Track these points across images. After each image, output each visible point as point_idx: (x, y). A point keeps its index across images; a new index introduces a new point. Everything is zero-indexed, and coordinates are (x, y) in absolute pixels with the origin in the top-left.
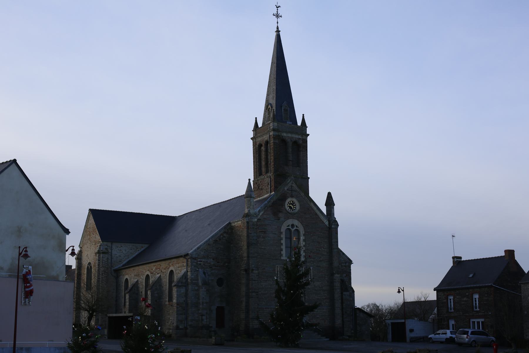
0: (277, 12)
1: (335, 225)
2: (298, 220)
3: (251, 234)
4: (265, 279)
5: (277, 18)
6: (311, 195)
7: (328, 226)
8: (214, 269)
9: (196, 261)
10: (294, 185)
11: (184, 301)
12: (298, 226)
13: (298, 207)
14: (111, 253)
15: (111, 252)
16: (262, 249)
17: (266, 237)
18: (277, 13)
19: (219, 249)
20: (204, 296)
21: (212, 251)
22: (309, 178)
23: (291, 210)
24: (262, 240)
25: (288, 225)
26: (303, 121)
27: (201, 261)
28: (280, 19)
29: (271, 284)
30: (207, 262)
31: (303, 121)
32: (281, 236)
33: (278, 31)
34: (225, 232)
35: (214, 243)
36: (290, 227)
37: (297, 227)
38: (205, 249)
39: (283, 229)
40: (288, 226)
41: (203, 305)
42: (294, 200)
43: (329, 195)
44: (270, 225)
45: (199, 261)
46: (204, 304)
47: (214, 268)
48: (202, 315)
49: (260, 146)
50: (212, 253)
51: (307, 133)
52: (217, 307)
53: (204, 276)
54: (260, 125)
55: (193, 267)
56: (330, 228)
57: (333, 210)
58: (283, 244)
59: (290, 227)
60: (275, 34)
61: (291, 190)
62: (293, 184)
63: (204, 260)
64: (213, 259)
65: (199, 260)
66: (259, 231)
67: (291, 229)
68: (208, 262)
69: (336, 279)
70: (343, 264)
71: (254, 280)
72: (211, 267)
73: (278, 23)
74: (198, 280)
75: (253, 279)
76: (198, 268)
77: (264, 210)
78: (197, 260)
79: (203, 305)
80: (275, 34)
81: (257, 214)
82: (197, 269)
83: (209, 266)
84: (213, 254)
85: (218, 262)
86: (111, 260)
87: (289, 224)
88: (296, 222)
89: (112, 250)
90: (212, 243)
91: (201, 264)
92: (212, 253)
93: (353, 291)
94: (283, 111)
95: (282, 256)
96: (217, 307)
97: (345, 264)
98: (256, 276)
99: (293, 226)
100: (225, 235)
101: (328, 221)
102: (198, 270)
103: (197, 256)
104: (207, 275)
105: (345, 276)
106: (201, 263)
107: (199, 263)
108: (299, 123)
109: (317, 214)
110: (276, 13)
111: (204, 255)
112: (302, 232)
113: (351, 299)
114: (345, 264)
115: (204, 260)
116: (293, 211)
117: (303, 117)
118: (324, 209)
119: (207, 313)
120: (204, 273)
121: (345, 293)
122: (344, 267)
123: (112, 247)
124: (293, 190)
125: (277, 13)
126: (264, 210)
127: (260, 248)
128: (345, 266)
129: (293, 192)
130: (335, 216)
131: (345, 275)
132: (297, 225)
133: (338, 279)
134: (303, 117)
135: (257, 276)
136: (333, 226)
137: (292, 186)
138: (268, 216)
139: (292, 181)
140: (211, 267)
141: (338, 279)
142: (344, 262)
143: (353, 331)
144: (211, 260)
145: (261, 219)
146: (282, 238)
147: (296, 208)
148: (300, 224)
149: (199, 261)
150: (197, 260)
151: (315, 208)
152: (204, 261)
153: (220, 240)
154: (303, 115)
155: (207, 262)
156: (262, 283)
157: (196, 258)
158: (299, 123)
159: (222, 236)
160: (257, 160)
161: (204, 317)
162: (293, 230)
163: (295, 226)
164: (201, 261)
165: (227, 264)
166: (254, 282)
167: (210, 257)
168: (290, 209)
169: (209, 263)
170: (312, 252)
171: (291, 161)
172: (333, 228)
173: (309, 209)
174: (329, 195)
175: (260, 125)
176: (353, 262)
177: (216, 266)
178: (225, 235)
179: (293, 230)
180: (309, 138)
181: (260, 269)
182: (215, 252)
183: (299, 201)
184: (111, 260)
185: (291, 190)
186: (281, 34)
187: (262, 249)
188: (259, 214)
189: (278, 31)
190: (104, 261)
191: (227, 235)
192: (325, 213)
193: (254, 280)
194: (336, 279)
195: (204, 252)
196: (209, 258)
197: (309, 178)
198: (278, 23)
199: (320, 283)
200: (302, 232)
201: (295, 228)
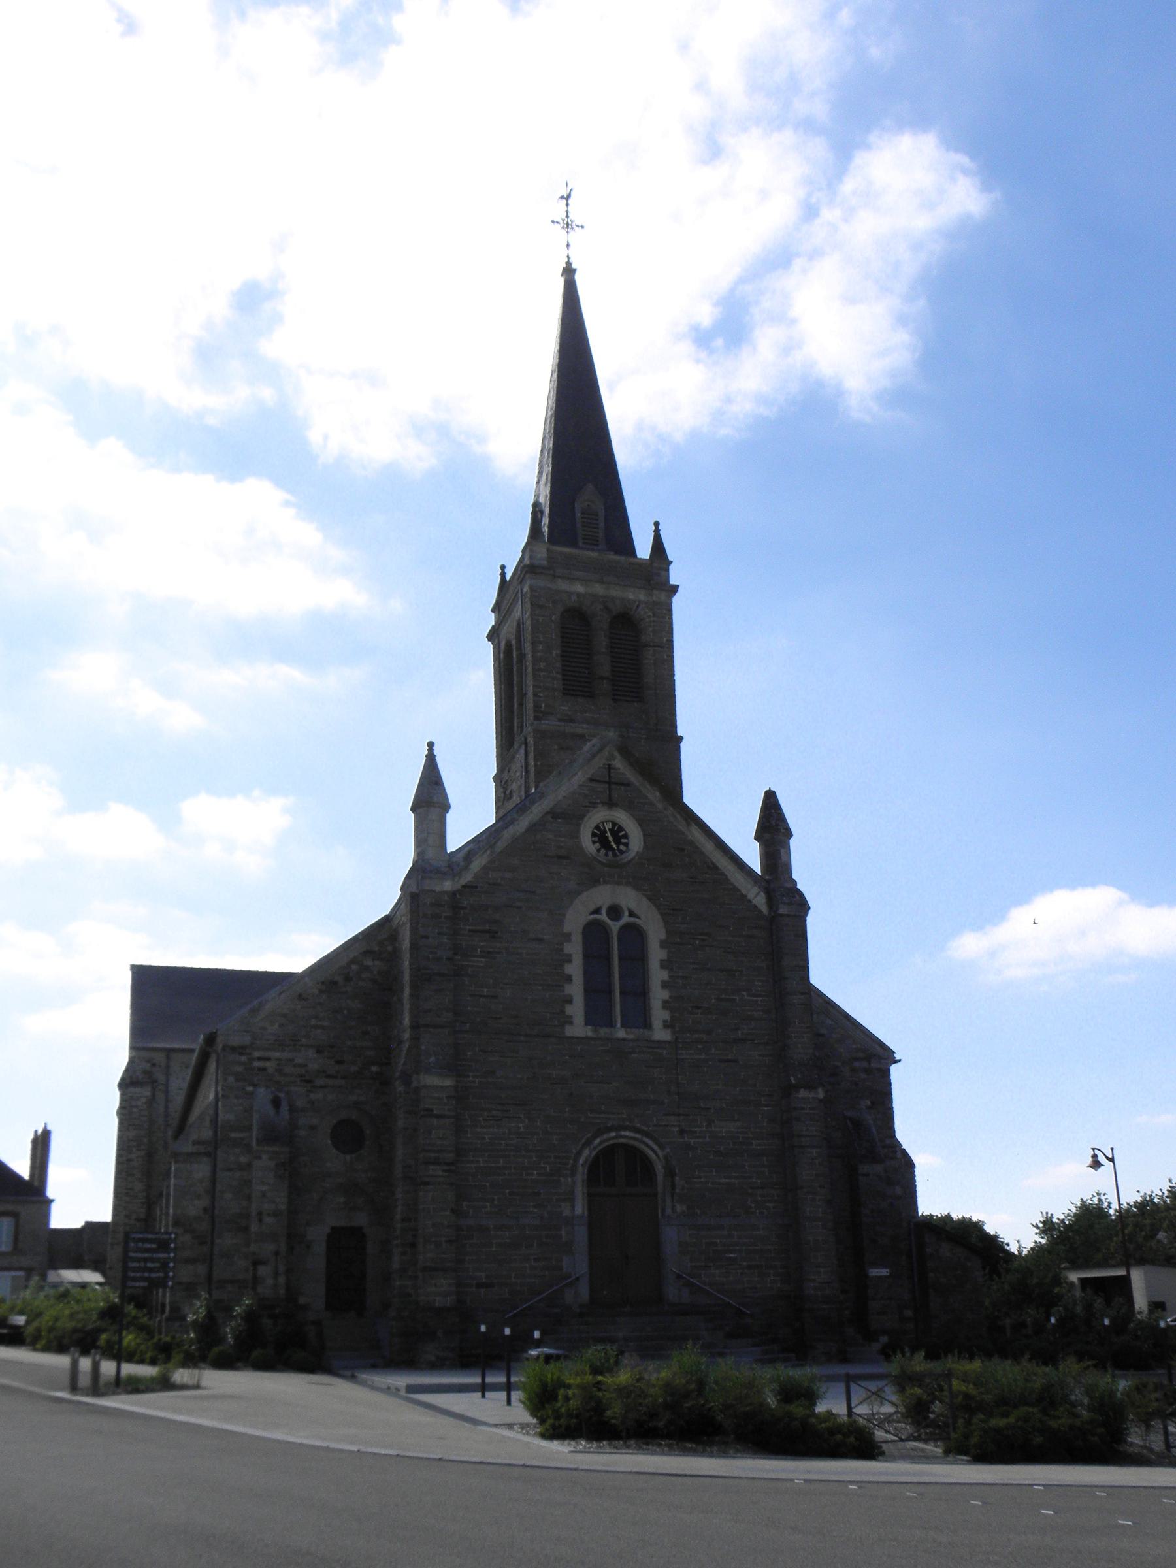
0: (567, 212)
1: (790, 904)
2: (637, 888)
3: (427, 937)
4: (494, 1113)
5: (568, 232)
6: (691, 799)
7: (765, 910)
8: (321, 1087)
9: (243, 1059)
10: (619, 763)
11: (205, 1210)
12: (637, 912)
13: (636, 841)
14: (167, 1085)
15: (168, 1080)
16: (484, 996)
17: (499, 953)
18: (567, 216)
19: (345, 1012)
20: (264, 1188)
21: (313, 1022)
22: (681, 738)
23: (610, 853)
24: (482, 962)
25: (592, 907)
26: (658, 546)
27: (269, 1059)
28: (575, 236)
29: (522, 1130)
30: (292, 1060)
31: (658, 546)
32: (562, 950)
33: (569, 272)
34: (367, 953)
35: (321, 991)
36: (604, 917)
37: (632, 914)
38: (285, 1016)
39: (576, 918)
40: (597, 911)
41: (260, 1221)
42: (623, 817)
43: (771, 804)
44: (519, 908)
45: (259, 1059)
46: (268, 1220)
47: (319, 1082)
48: (256, 1263)
49: (509, 646)
50: (316, 1027)
51: (671, 583)
52: (333, 1228)
53: (271, 1111)
54: (508, 577)
55: (231, 1079)
56: (774, 918)
57: (782, 851)
58: (574, 978)
59: (604, 917)
60: (560, 284)
61: (605, 782)
62: (613, 757)
63: (277, 1055)
64: (319, 1051)
65: (257, 1054)
66: (470, 931)
67: (609, 921)
68: (298, 1061)
69: (803, 1109)
70: (857, 1064)
71: (438, 1116)
72: (309, 1081)
73: (568, 245)
74: (249, 1128)
75: (432, 1110)
76: (255, 1085)
77: (488, 852)
78: (250, 1054)
79: (260, 1221)
80: (561, 282)
81: (458, 865)
82: (250, 1089)
83: (302, 1076)
84: (319, 1031)
85: (339, 1062)
86: (166, 1107)
87: (598, 906)
88: (628, 898)
89: (167, 1074)
90: (316, 991)
91: (264, 1069)
92: (316, 1027)
94: (578, 515)
95: (571, 1023)
96: (333, 1228)
97: (865, 1064)
98: (445, 1101)
99: (615, 912)
100: (368, 962)
101: (762, 894)
102: (252, 1093)
103: (247, 1040)
104: (285, 1108)
105: (869, 1108)
106: (268, 1064)
107: (257, 1064)
108: (643, 550)
109: (717, 868)
110: (564, 217)
111: (279, 1036)
112: (655, 931)
114: (865, 1064)
115: (277, 1055)
116: (615, 855)
117: (657, 532)
118: (751, 855)
119: (277, 1253)
120: (276, 1103)
121: (864, 1168)
122: (863, 1076)
123: (168, 1067)
124: (613, 780)
125: (567, 216)
126: (488, 852)
127: (471, 995)
128: (867, 1071)
129: (613, 786)
130: (794, 877)
131: (869, 1103)
132: (633, 906)
133: (810, 1109)
134: (657, 532)
135: (448, 1097)
136: (783, 910)
137: (610, 768)
138: (508, 875)
139: (608, 749)
140: (309, 1081)
141: (810, 1109)
142: (861, 1055)
143: (909, 1313)
144: (311, 1053)
145: (476, 887)
146: (570, 955)
147: (630, 846)
148: (645, 902)
149: (259, 1059)
150: (250, 1054)
151: (708, 847)
152: (278, 1059)
153: (348, 979)
154: (657, 524)
155: (293, 1060)
156: (479, 1130)
157: (243, 1047)
158: (643, 550)
159: (354, 967)
161: (262, 1271)
162: (615, 927)
163: (626, 913)
164: (269, 1059)
165: (374, 1069)
166: (435, 1121)
167: (304, 1041)
168: (603, 851)
169: (300, 1066)
170: (698, 1008)
171: (602, 678)
172: (782, 915)
173: (683, 850)
174: (771, 804)
175: (508, 577)
176: (897, 1056)
177: (329, 1076)
178: (368, 962)
179: (615, 927)
180: (677, 602)
181: (471, 1074)
182: (326, 1024)
183: (641, 822)
184: (166, 1107)
185: (605, 782)
186: (578, 278)
187: (484, 996)
188: (467, 868)
189: (569, 272)
190: (135, 1110)
191: (377, 963)
192: (755, 864)
193: (438, 1116)
194: (803, 1109)
195: (281, 1026)
196: (302, 1045)
197: (681, 738)
198: (568, 245)
199: (739, 1124)
200: (655, 931)
201: (626, 919)
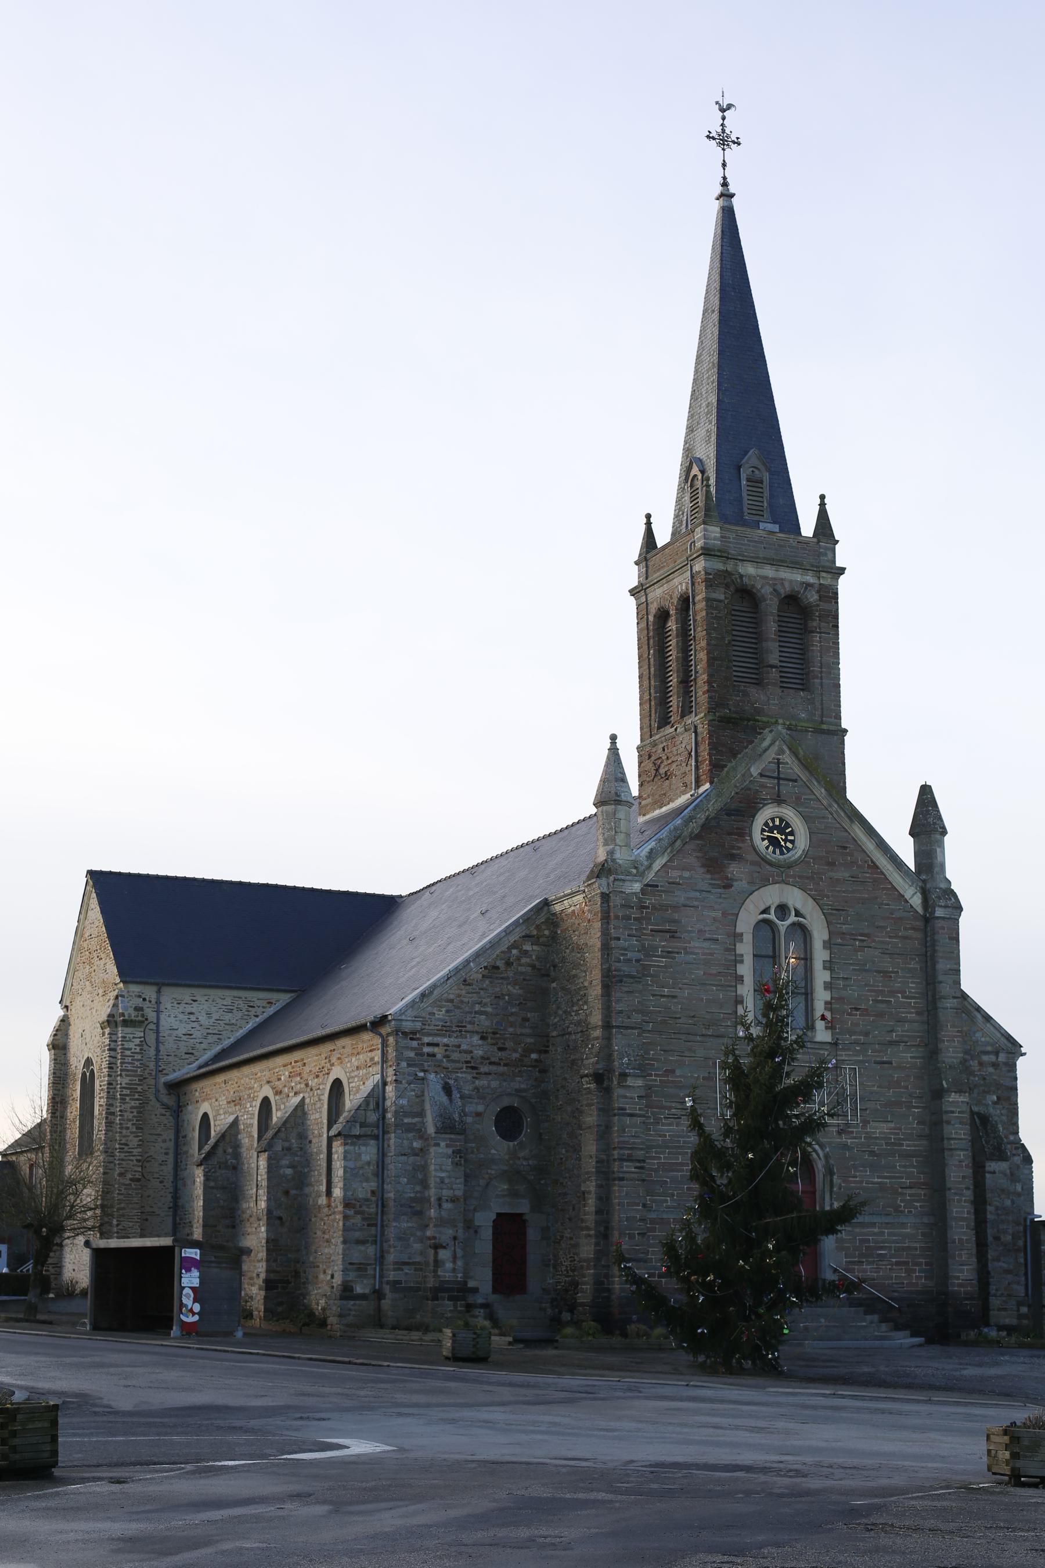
1: (946, 907)
3: (618, 939)
5: (724, 150)
6: (853, 794)
7: (920, 910)
8: (486, 1074)
9: (415, 1044)
10: (787, 758)
11: (373, 1192)
12: (803, 911)
13: (802, 840)
14: (158, 1024)
15: (158, 1018)
16: (664, 996)
17: (678, 953)
19: (507, 997)
20: (443, 1175)
21: (477, 1008)
22: (845, 731)
23: (778, 851)
25: (762, 908)
26: (823, 517)
27: (437, 1045)
28: (732, 154)
30: (459, 1046)
31: (823, 517)
32: (735, 950)
33: (726, 195)
34: (527, 937)
37: (798, 914)
38: (452, 1001)
39: (747, 921)
40: (766, 911)
41: (440, 1206)
42: (789, 813)
43: (926, 798)
45: (429, 1044)
46: (446, 1206)
47: (484, 1069)
48: (436, 1247)
49: (663, 616)
52: (499, 1215)
53: (444, 1099)
54: (663, 537)
55: (404, 1064)
56: (928, 919)
57: (938, 850)
58: (745, 979)
59: (772, 916)
62: (781, 752)
63: (445, 1040)
64: (483, 1038)
65: (426, 1040)
66: (652, 930)
68: (464, 1047)
69: (953, 1112)
70: (985, 1058)
71: (631, 1115)
72: (473, 1068)
73: (724, 165)
74: (421, 1114)
76: (425, 1071)
79: (440, 1206)
80: (715, 206)
82: (421, 1074)
83: (467, 1062)
84: (483, 1017)
85: (500, 1049)
86: (158, 1050)
87: (768, 905)
88: (796, 898)
89: (158, 1012)
90: (480, 976)
91: (434, 1055)
93: (1028, 1160)
94: (744, 482)
96: (499, 1215)
97: (993, 1058)
99: (783, 910)
100: (527, 947)
101: (919, 894)
102: (423, 1079)
103: (418, 1025)
104: (456, 1095)
105: (995, 1103)
106: (436, 1050)
107: (426, 1050)
108: (808, 527)
109: (877, 867)
110: (719, 130)
112: (819, 934)
113: (1019, 1188)
114: (993, 1058)
115: (445, 1040)
116: (782, 853)
117: (822, 505)
118: (905, 850)
119: (455, 1238)
120: (447, 1090)
121: (991, 1166)
122: (991, 1070)
123: (158, 1003)
124: (782, 776)
125: (723, 131)
126: (669, 851)
127: (654, 995)
128: (995, 1065)
129: (781, 782)
130: (949, 875)
131: (995, 1098)
132: (799, 906)
133: (959, 1112)
136: (939, 912)
137: (779, 763)
138: (686, 874)
139: (777, 743)
140: (473, 1068)
141: (959, 1112)
142: (989, 1048)
143: (1024, 1310)
144: (476, 1039)
145: (657, 886)
149: (429, 1044)
151: (870, 846)
152: (447, 1045)
153: (508, 964)
154: (822, 497)
155: (459, 1046)
157: (414, 1033)
158: (808, 527)
159: (514, 952)
160: (652, 669)
161: (443, 1254)
162: (783, 925)
163: (793, 913)
164: (437, 1045)
165: (534, 1056)
166: (628, 1120)
167: (469, 1027)
168: (771, 848)
169: (466, 1052)
170: (857, 1009)
171: (772, 666)
172: (938, 918)
173: (845, 848)
174: (926, 798)
175: (663, 537)
176: (1023, 1050)
177: (491, 1063)
178: (527, 947)
180: (843, 584)
182: (489, 1009)
183: (807, 819)
184: (158, 1050)
187: (664, 996)
188: (649, 867)
189: (726, 195)
190: (128, 1053)
191: (535, 947)
192: (910, 862)
193: (631, 1115)
194: (953, 1112)
195: (447, 1011)
197: (845, 731)
198: (724, 165)
199: (892, 1125)
200: (819, 934)
201: (793, 918)
